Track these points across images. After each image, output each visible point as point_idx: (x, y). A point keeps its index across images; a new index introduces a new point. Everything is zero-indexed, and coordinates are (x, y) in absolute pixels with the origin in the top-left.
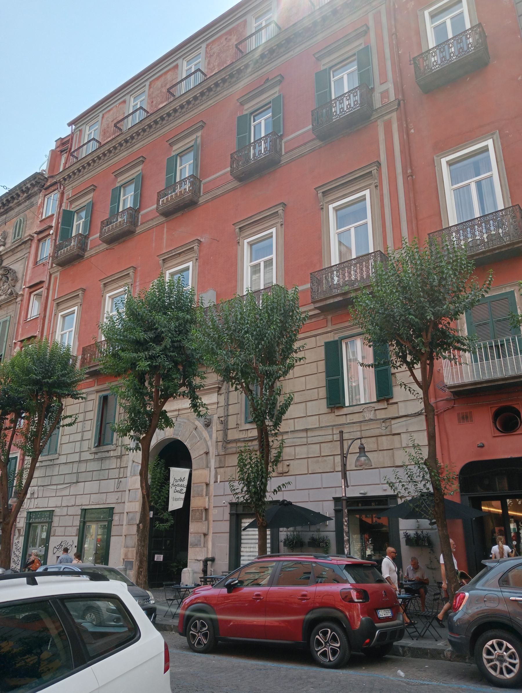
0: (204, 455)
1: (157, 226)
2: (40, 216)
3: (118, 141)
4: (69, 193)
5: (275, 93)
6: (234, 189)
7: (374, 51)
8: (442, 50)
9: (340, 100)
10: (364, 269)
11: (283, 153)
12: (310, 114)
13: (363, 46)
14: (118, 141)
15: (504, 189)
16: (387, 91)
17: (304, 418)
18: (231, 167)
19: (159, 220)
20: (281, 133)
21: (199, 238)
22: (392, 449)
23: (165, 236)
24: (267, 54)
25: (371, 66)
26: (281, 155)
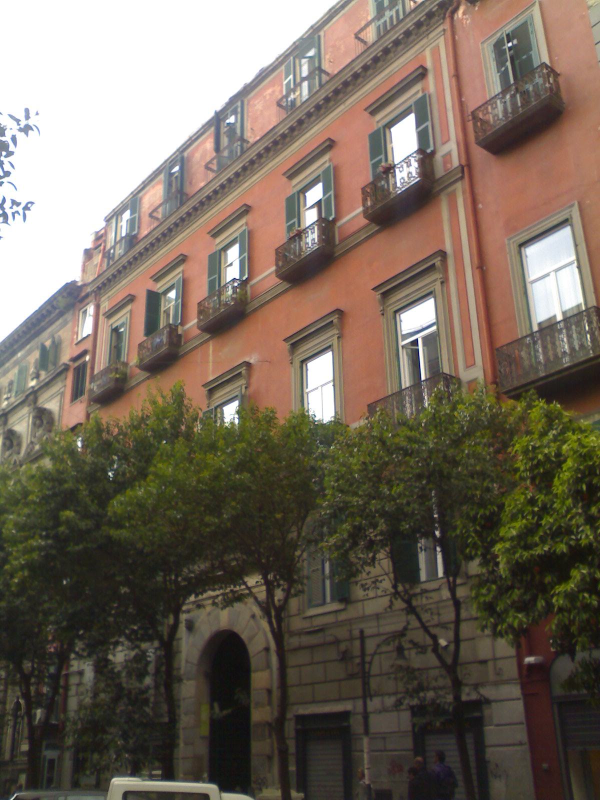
0: (263, 653)
1: (202, 344)
2: (75, 337)
3: (154, 235)
4: (106, 306)
5: (417, 92)
6: (286, 291)
7: (434, 99)
8: (485, 112)
9: (483, 111)
10: (549, 346)
11: (337, 242)
12: (274, 252)
13: (420, 95)
14: (154, 235)
15: (525, 307)
16: (449, 154)
17: (374, 600)
18: (364, 205)
19: (203, 337)
20: (432, 148)
21: (247, 359)
22: (473, 639)
23: (211, 358)
24: (413, 29)
25: (217, 276)
26: (334, 246)
